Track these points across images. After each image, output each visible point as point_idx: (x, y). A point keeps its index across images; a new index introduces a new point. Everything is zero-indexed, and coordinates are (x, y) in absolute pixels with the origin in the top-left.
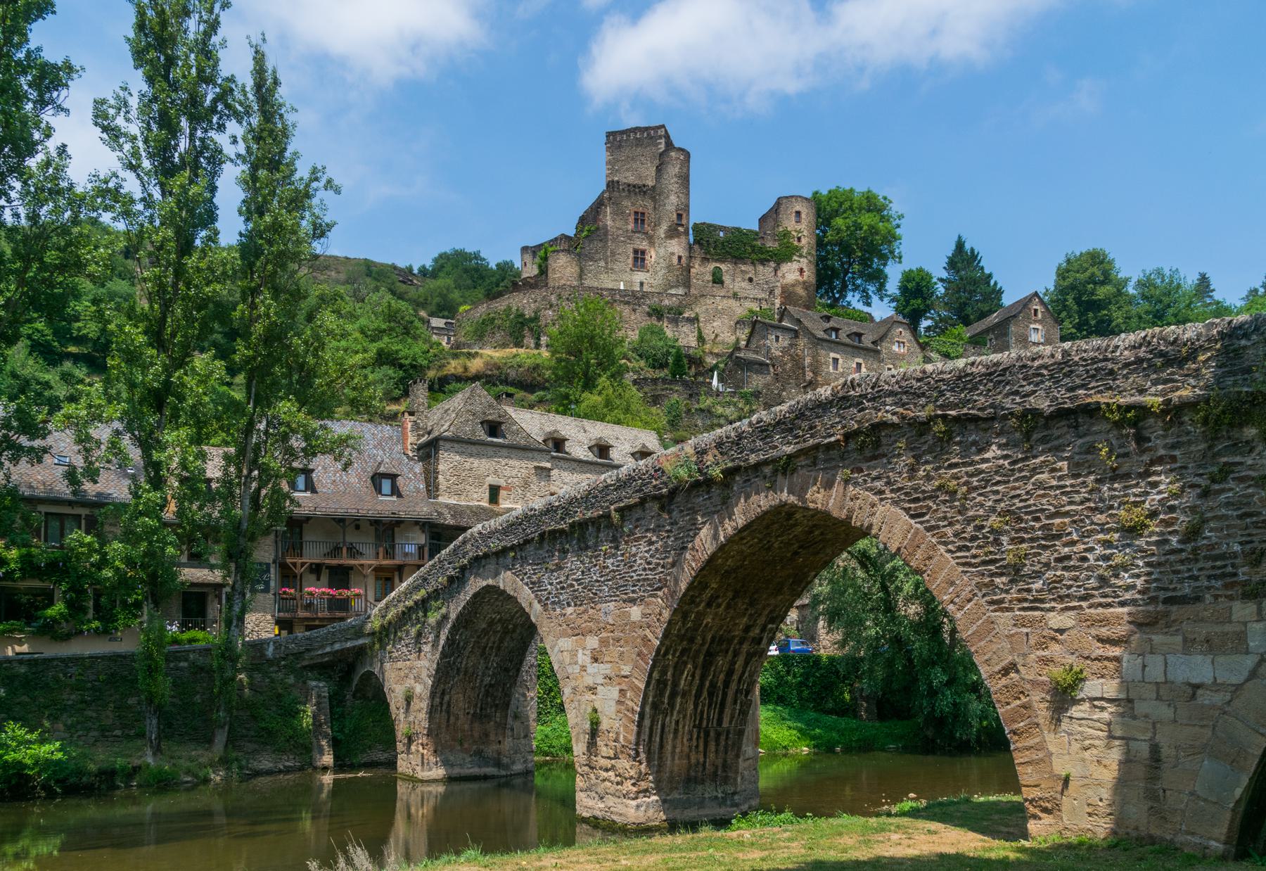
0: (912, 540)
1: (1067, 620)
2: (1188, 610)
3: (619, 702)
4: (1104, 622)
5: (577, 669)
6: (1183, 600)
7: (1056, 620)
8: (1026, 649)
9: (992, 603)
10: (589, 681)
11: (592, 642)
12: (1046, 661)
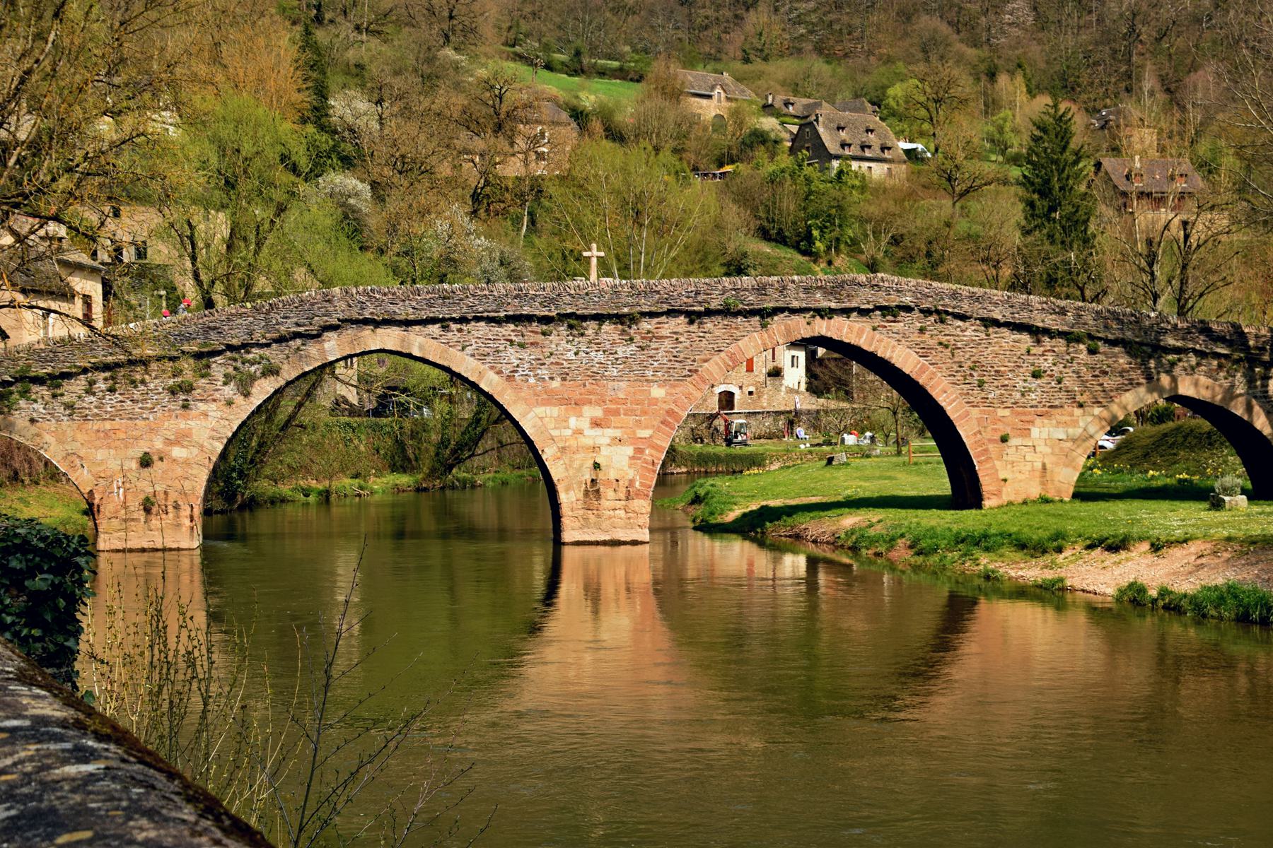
0: (921, 368)
1: (1007, 412)
2: (1059, 410)
3: (632, 458)
4: (1024, 414)
5: (569, 432)
6: (1055, 407)
7: (1002, 412)
8: (986, 424)
9: (968, 403)
10: (589, 442)
11: (598, 412)
12: (995, 430)
